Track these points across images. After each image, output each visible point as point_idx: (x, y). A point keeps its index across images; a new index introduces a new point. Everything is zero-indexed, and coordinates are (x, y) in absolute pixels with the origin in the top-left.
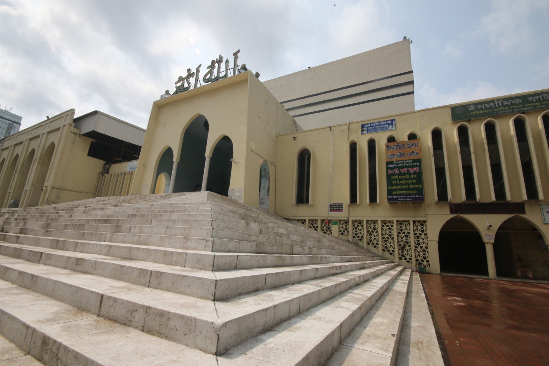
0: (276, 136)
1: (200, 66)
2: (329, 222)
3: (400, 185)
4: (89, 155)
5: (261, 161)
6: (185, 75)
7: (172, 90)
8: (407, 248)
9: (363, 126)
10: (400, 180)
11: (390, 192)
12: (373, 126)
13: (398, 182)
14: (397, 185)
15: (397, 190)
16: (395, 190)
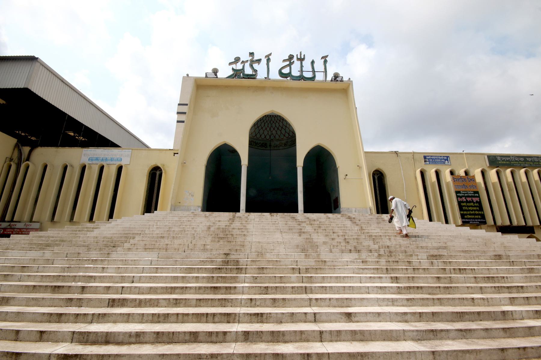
1: (270, 54)
3: (469, 210)
6: (245, 57)
7: (225, 72)
9: (425, 157)
10: (468, 207)
16: (466, 215)
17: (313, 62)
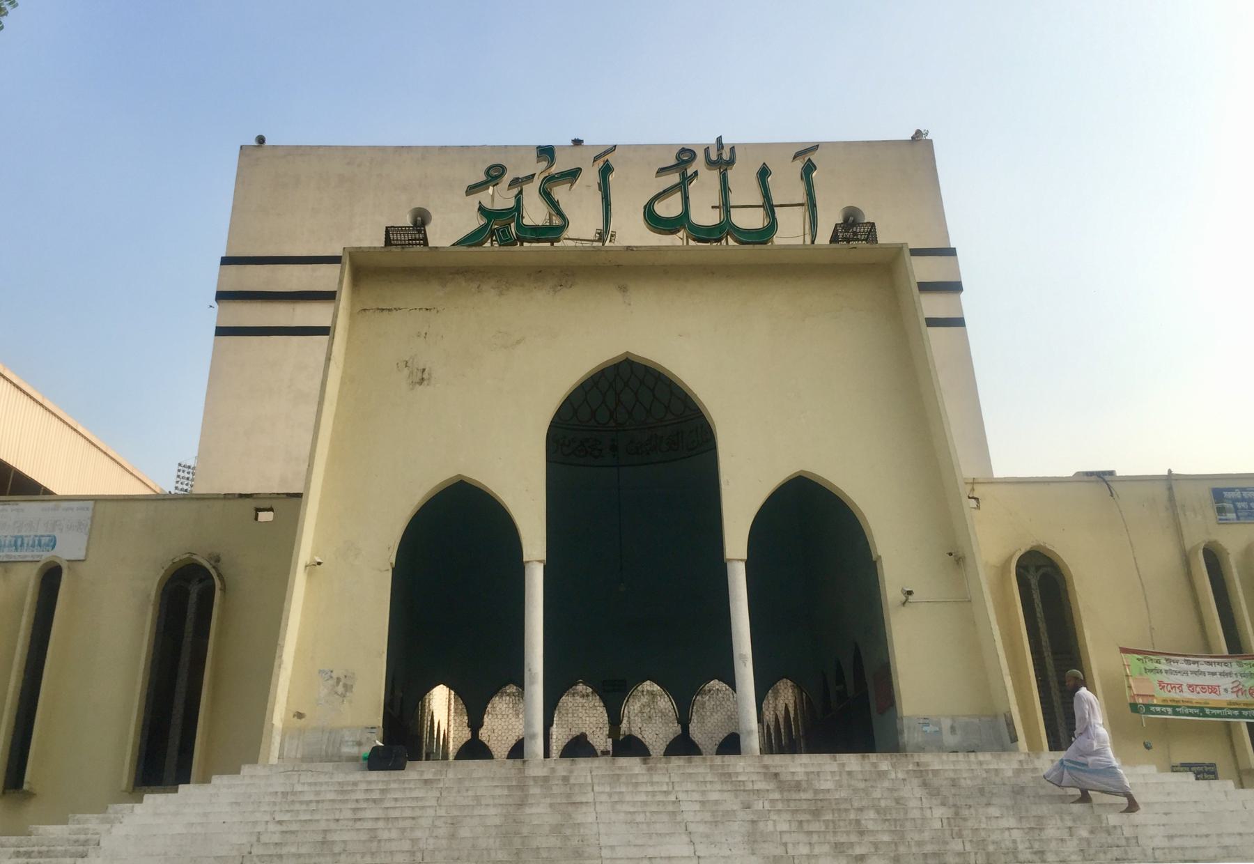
17: (764, 173)
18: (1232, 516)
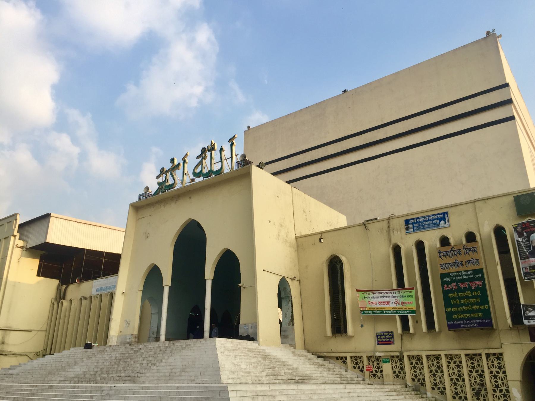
0: (297, 238)
2: (378, 360)
3: (462, 305)
4: (38, 275)
5: (280, 278)
8: (483, 392)
9: (407, 222)
10: (460, 298)
11: (449, 316)
12: (420, 222)
13: (458, 302)
14: (457, 306)
15: (459, 312)
16: (456, 313)
18: (412, 230)
